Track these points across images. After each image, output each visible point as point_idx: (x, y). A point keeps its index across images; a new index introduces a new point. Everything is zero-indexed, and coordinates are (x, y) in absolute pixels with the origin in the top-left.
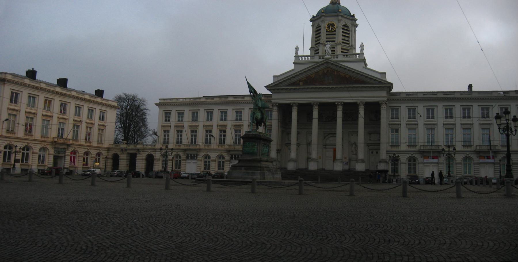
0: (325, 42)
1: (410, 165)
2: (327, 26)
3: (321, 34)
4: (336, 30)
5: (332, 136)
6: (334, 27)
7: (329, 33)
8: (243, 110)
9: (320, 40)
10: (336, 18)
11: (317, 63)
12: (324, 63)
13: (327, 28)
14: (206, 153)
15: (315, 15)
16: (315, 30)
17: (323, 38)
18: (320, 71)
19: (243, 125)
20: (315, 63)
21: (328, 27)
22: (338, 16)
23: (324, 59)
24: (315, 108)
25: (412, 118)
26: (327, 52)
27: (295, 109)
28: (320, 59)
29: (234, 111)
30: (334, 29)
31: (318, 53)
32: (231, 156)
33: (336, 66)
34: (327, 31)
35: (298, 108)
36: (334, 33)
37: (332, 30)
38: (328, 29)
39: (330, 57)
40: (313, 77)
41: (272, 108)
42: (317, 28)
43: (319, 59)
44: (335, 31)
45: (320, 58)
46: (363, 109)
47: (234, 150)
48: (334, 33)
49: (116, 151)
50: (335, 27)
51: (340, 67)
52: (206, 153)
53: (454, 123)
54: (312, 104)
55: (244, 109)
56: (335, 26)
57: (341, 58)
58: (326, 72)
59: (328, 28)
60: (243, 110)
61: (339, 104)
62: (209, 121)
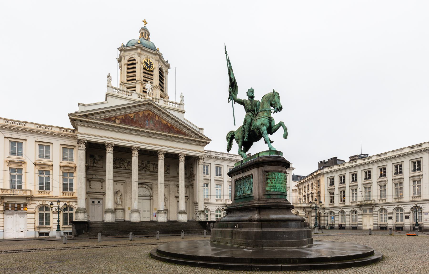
0: (142, 80)
1: (41, 214)
2: (144, 62)
3: (136, 70)
4: (154, 70)
5: (141, 187)
6: (152, 66)
7: (146, 71)
8: (24, 142)
9: (135, 76)
10: (154, 56)
11: (137, 102)
12: (147, 103)
13: (144, 64)
14: (353, 209)
15: (125, 45)
16: (126, 62)
17: (139, 74)
18: (140, 112)
19: (25, 163)
20: (135, 101)
21: (145, 63)
22: (156, 54)
23: (144, 100)
24: (135, 153)
25: (205, 173)
26: (149, 92)
27: (111, 151)
28: (139, 98)
29: (8, 140)
30: (151, 69)
31: (135, 91)
32: (5, 204)
33: (159, 110)
34: (144, 69)
35: (113, 150)
36: (151, 73)
37: (149, 69)
38: (145, 67)
39: (151, 98)
40: (132, 117)
41: (75, 146)
42: (129, 61)
43: (138, 98)
44: (152, 71)
45: (139, 97)
46: (163, 159)
47: (14, 197)
48: (151, 73)
49: (354, 208)
50: (153, 67)
51: (164, 113)
52: (353, 209)
53: (222, 180)
54: (132, 148)
55: (26, 140)
56: (152, 65)
57: (161, 103)
58: (146, 114)
59: (145, 65)
60: (24, 142)
61: (162, 153)
62: (15, 155)
